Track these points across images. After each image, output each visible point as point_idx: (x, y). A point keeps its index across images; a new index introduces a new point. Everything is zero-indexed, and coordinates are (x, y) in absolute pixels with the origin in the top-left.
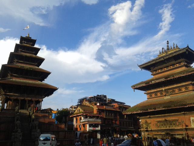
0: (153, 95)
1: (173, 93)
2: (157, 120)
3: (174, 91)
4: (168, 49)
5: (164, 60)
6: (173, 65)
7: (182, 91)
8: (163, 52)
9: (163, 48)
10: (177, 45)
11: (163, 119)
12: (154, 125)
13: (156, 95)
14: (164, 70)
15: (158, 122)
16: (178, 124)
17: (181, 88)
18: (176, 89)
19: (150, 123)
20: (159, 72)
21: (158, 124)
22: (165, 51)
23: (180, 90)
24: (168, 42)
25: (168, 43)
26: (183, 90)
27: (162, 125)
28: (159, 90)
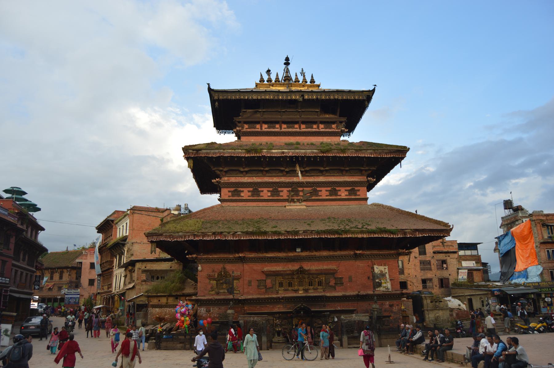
0: (246, 193)
2: (266, 269)
4: (287, 78)
5: (301, 99)
6: (309, 123)
8: (269, 80)
9: (268, 72)
10: (312, 76)
11: (294, 267)
14: (281, 128)
15: (269, 274)
16: (332, 283)
17: (337, 189)
18: (324, 189)
19: (238, 278)
20: (264, 130)
21: (269, 281)
22: (277, 80)
23: (334, 192)
24: (287, 59)
25: (287, 63)
26: (343, 194)
27: (281, 285)
28: (267, 179)
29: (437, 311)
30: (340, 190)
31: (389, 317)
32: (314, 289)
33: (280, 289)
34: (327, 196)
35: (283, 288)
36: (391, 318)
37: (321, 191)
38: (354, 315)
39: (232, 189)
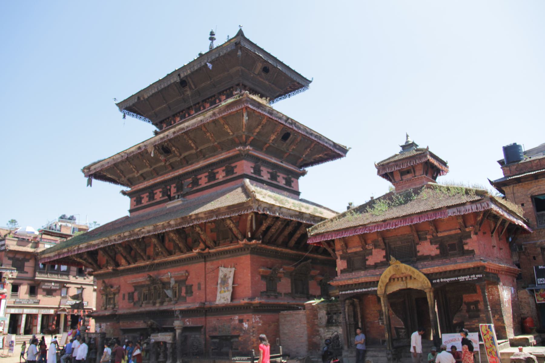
0: (145, 201)
1: (192, 187)
3: (196, 182)
7: (218, 179)
12: (124, 298)
13: (152, 197)
21: (136, 294)
23: (212, 177)
26: (221, 177)
27: (146, 298)
28: (159, 179)
29: (334, 328)
30: (218, 172)
31: (238, 336)
32: (168, 301)
33: (144, 302)
34: (206, 183)
35: (146, 301)
36: (240, 339)
37: (201, 178)
38: (159, 334)
39: (135, 198)
